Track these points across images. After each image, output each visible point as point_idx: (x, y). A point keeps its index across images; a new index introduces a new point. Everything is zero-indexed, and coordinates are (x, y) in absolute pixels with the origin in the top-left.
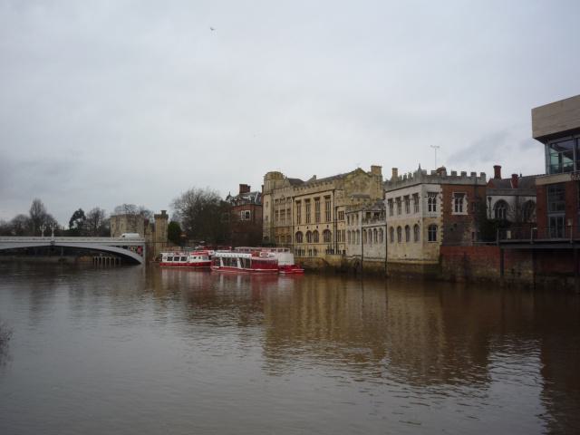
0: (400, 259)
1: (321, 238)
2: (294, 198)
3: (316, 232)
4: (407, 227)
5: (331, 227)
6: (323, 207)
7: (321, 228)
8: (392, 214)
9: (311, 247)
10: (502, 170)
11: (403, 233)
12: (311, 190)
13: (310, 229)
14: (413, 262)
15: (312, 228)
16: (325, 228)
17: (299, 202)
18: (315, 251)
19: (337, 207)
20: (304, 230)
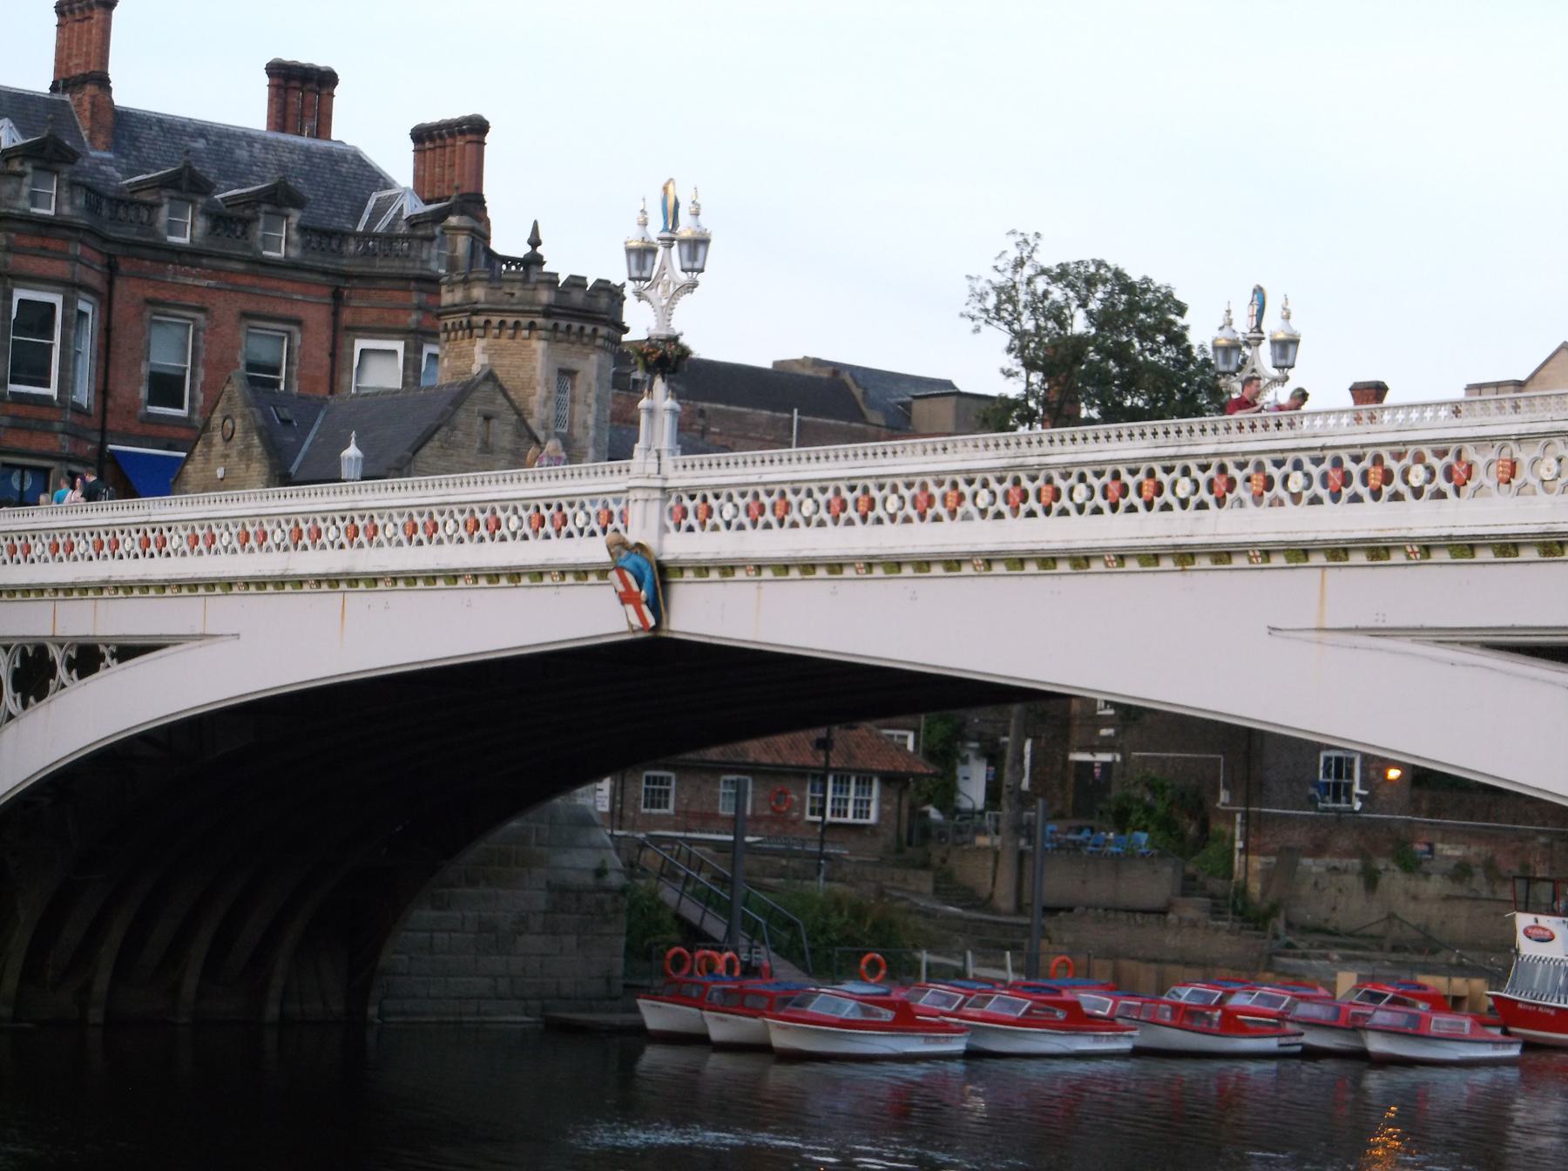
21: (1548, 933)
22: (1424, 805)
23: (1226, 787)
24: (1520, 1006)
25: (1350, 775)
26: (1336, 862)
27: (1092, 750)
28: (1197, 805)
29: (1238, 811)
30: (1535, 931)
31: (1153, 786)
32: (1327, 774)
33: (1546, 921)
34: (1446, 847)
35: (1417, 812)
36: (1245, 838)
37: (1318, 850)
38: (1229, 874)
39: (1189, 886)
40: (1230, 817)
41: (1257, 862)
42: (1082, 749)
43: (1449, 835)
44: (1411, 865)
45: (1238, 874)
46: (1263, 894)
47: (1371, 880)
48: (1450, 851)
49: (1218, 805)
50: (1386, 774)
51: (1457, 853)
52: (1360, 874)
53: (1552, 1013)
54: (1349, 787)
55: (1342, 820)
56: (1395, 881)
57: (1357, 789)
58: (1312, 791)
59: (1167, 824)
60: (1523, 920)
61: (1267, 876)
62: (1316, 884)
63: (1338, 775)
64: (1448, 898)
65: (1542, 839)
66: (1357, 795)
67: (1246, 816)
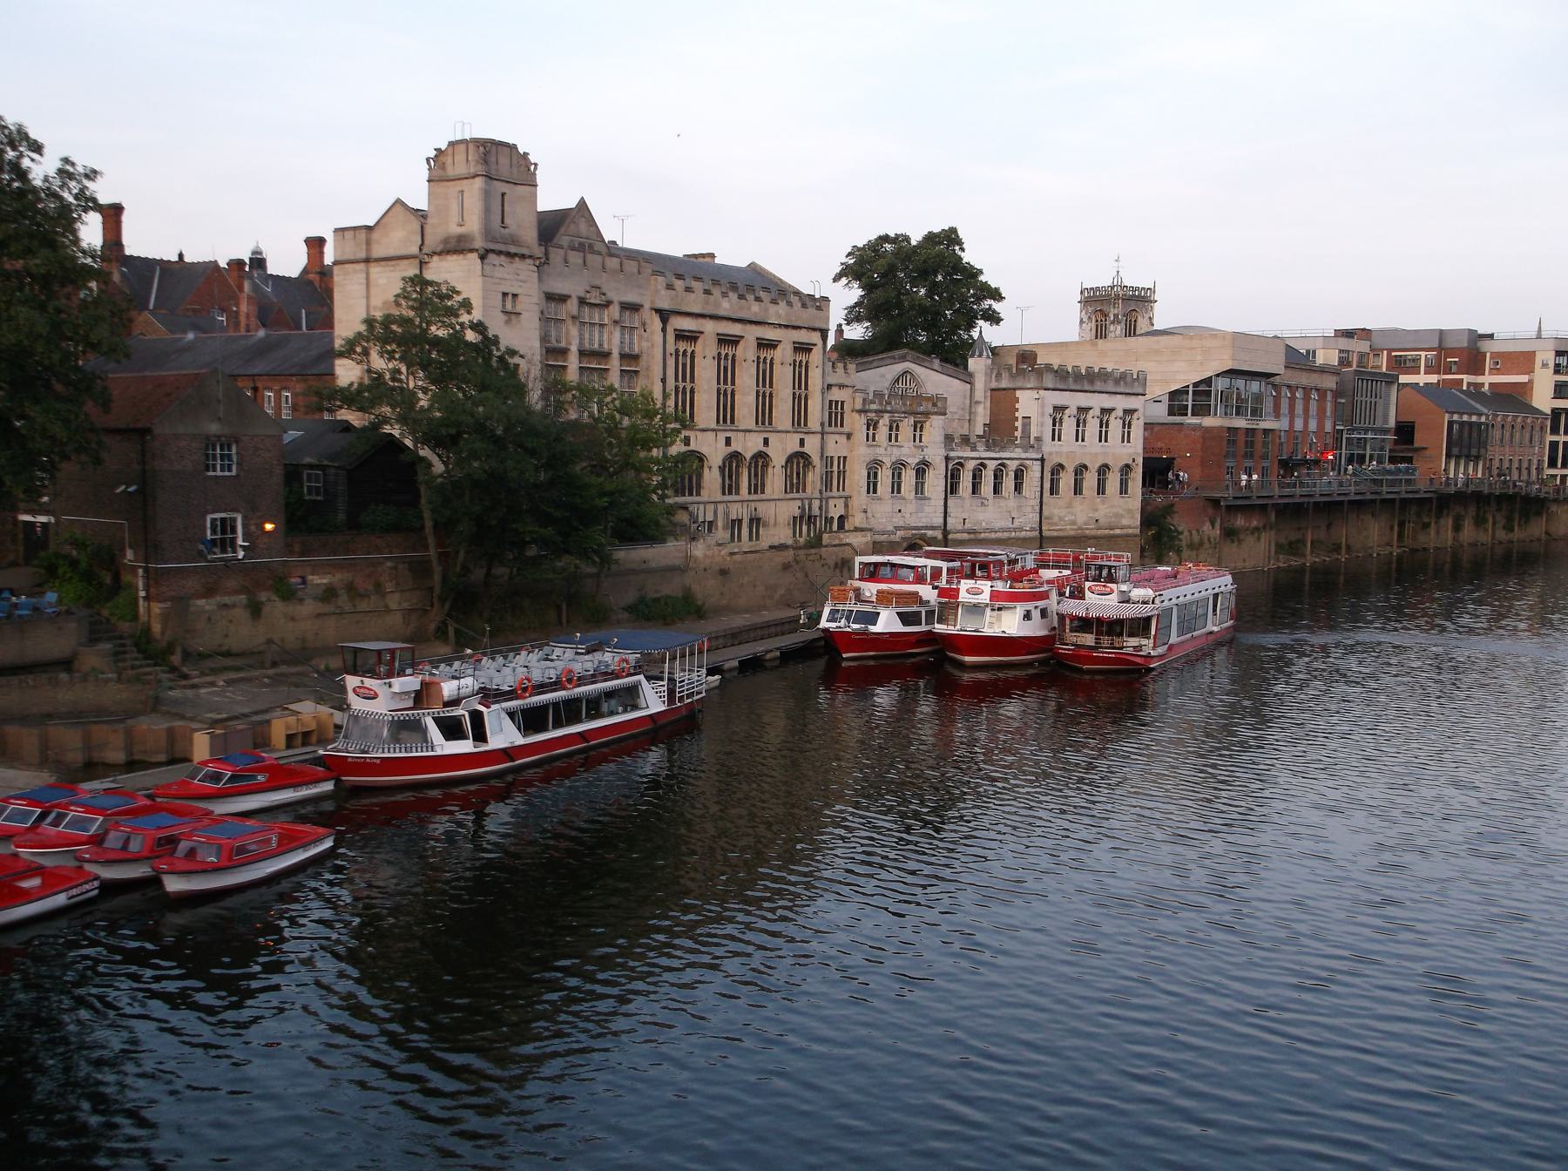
0: (1080, 529)
1: (775, 479)
2: (664, 315)
3: (761, 459)
4: (1104, 469)
5: (812, 446)
6: (783, 378)
7: (781, 448)
8: (1056, 436)
9: (736, 511)
10: (126, 219)
11: (1090, 480)
12: (754, 311)
13: (735, 447)
14: (1118, 532)
15: (749, 445)
16: (792, 444)
17: (691, 337)
18: (756, 521)
19: (830, 387)
20: (712, 448)
21: (372, 692)
22: (297, 548)
23: (131, 547)
24: (349, 760)
25: (234, 530)
26: (227, 600)
27: (33, 513)
28: (109, 559)
29: (141, 567)
30: (362, 690)
31: (79, 545)
32: (214, 531)
33: (369, 682)
34: (315, 577)
35: (291, 553)
36: (147, 589)
37: (209, 592)
38: (136, 617)
39: (96, 633)
40: (134, 569)
41: (157, 608)
42: (27, 512)
43: (317, 568)
44: (288, 595)
45: (143, 616)
46: (163, 633)
47: (255, 610)
48: (319, 580)
49: (126, 561)
50: (264, 528)
51: (325, 581)
52: (247, 606)
53: (378, 761)
54: (233, 541)
55: (230, 566)
56: (276, 608)
57: (240, 542)
58: (201, 547)
59: (89, 577)
60: (352, 681)
61: (165, 618)
62: (209, 619)
63: (224, 532)
64: (319, 615)
65: (389, 564)
66: (241, 546)
67: (146, 570)
